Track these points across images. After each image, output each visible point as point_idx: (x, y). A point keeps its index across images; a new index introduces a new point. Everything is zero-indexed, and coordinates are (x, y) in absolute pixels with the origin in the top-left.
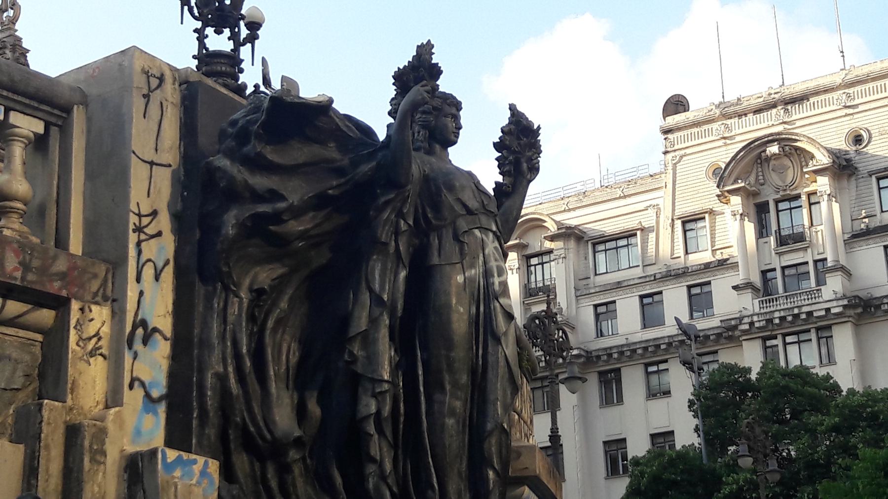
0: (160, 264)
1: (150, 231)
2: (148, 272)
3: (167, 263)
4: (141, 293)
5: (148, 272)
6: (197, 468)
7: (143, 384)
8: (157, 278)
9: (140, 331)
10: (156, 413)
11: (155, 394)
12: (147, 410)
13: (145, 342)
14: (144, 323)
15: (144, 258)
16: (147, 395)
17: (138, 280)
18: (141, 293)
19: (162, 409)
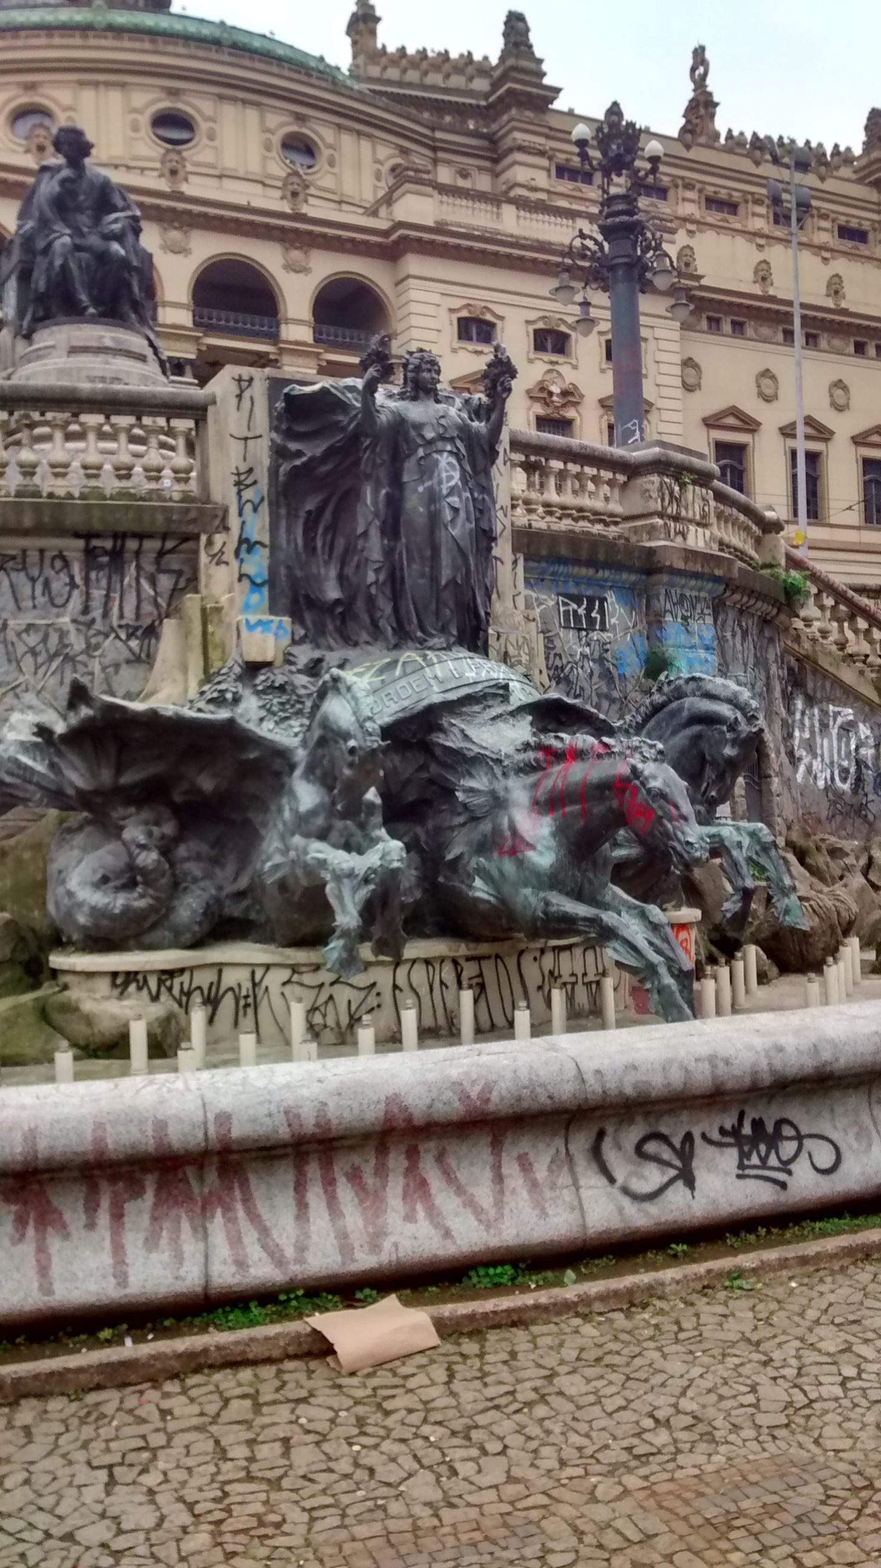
0: (257, 501)
1: (248, 482)
2: (248, 508)
3: (262, 499)
4: (243, 523)
5: (248, 508)
6: (274, 626)
7: (248, 577)
8: (255, 510)
9: (244, 546)
10: (261, 593)
11: (259, 581)
12: (252, 592)
13: (249, 550)
14: (247, 540)
15: (244, 500)
16: (253, 583)
17: (240, 514)
18: (243, 523)
19: (265, 590)
